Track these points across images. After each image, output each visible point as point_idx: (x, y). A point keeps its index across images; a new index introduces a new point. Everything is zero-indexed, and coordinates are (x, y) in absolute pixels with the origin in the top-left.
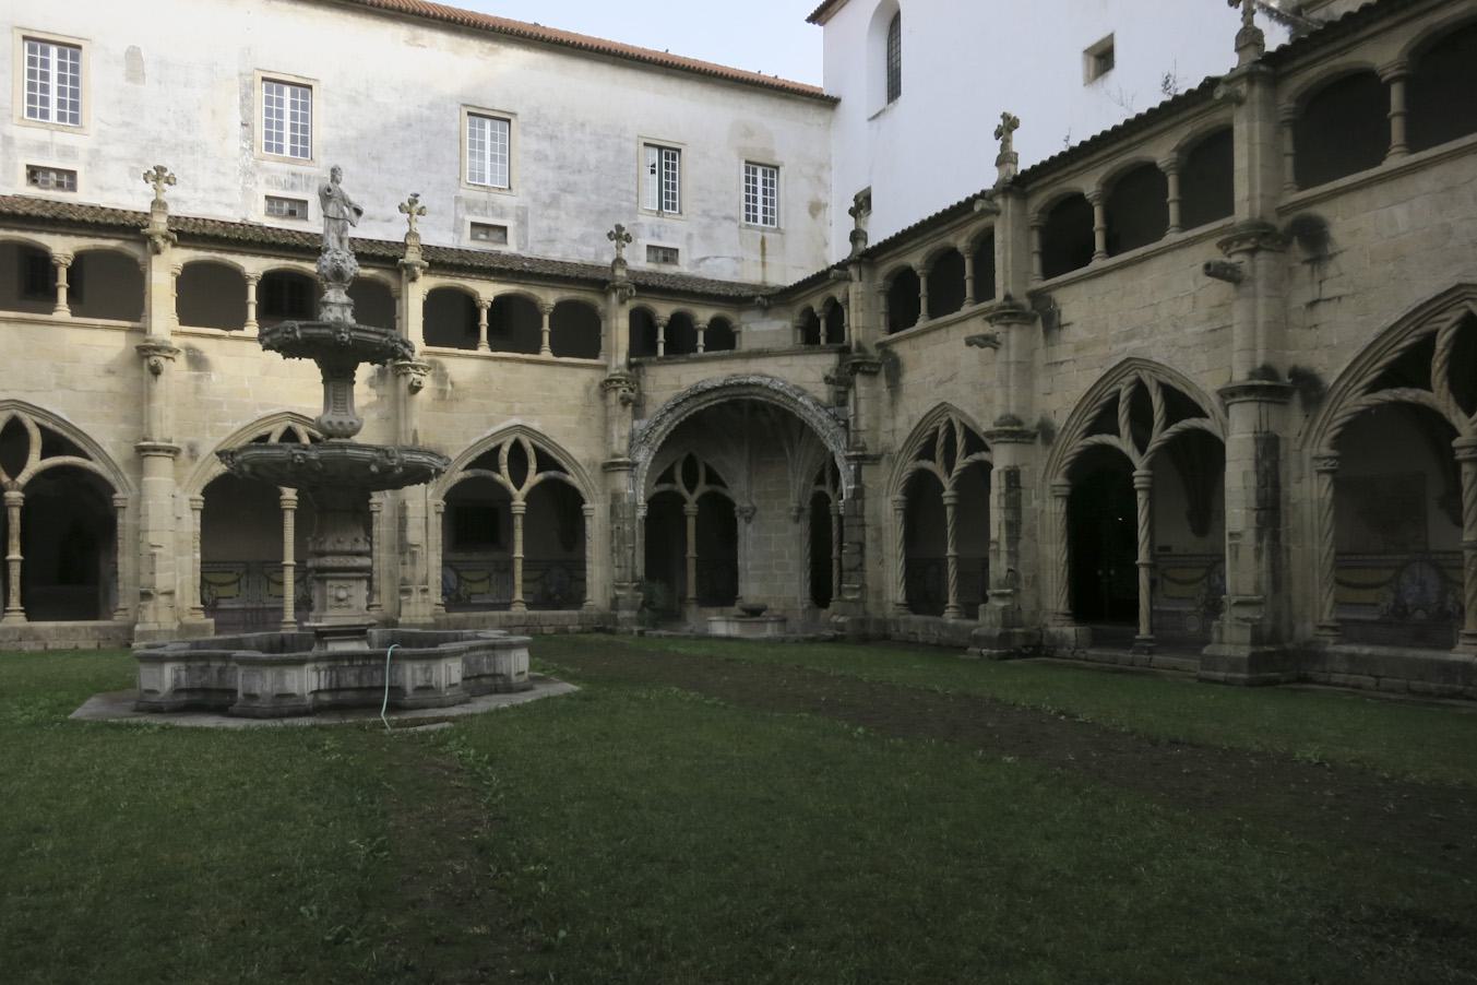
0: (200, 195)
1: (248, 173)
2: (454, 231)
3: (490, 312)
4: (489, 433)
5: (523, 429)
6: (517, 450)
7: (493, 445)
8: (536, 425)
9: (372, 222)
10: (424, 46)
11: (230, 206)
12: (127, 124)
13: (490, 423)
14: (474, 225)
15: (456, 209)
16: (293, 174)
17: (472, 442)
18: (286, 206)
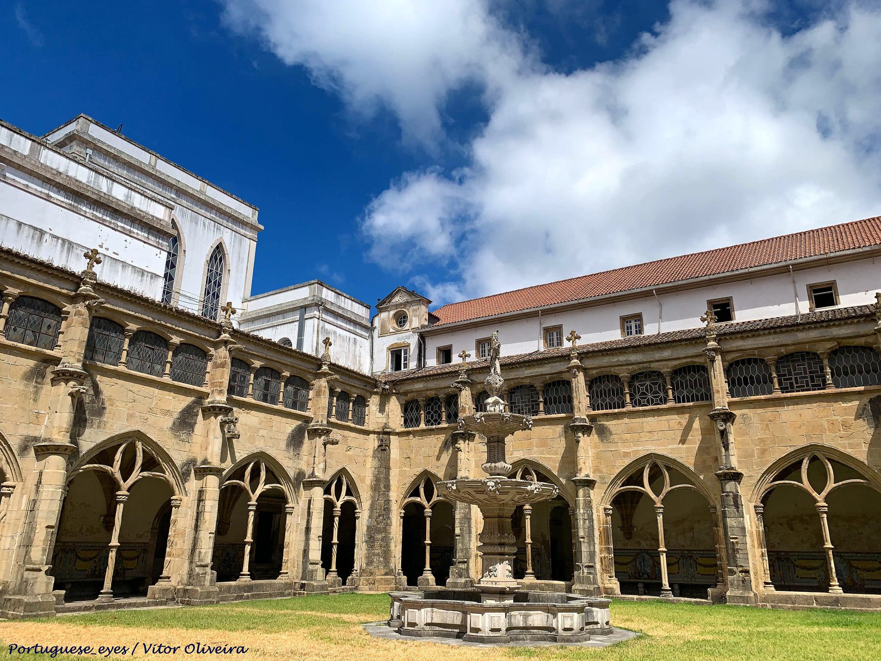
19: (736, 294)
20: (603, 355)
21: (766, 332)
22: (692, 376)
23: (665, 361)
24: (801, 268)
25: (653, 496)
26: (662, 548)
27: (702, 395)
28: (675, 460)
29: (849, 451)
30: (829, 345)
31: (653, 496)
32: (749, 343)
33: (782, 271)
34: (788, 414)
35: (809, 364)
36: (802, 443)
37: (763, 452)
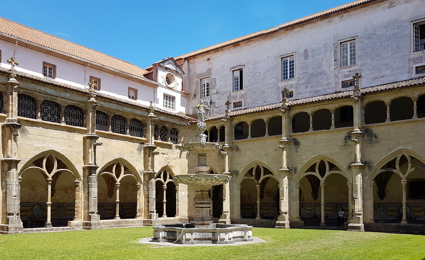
0: (323, 87)
1: (336, 76)
2: (409, 73)
3: (418, 102)
4: (390, 153)
5: (406, 150)
6: (322, 164)
7: (393, 158)
8: (410, 148)
9: (377, 79)
10: (395, 6)
11: (332, 88)
12: (304, 73)
13: (390, 151)
14: (416, 67)
15: (409, 64)
16: (350, 71)
17: (383, 158)
18: (349, 82)
19: (61, 66)
20: (32, 82)
21: (115, 102)
22: (73, 112)
23: (65, 99)
24: (93, 67)
25: (48, 174)
26: (49, 202)
27: (76, 123)
28: (63, 156)
29: (131, 162)
30: (133, 117)
31: (48, 174)
32: (106, 105)
33: (84, 64)
34: (114, 142)
35: (121, 122)
36: (117, 157)
37: (103, 158)
